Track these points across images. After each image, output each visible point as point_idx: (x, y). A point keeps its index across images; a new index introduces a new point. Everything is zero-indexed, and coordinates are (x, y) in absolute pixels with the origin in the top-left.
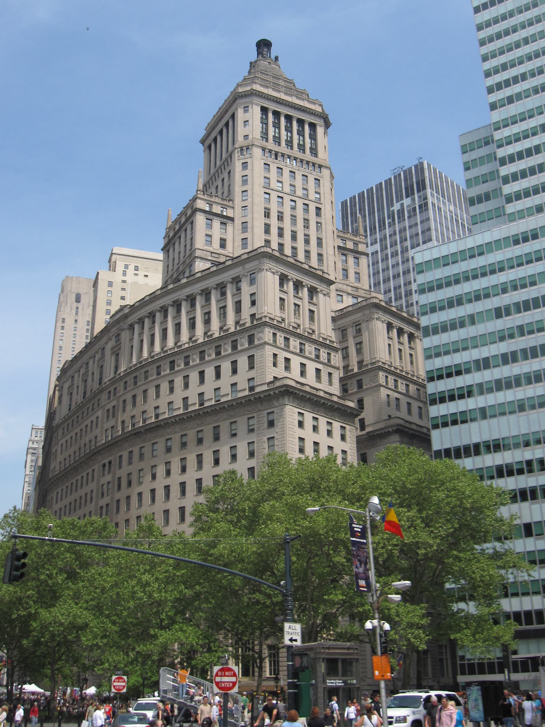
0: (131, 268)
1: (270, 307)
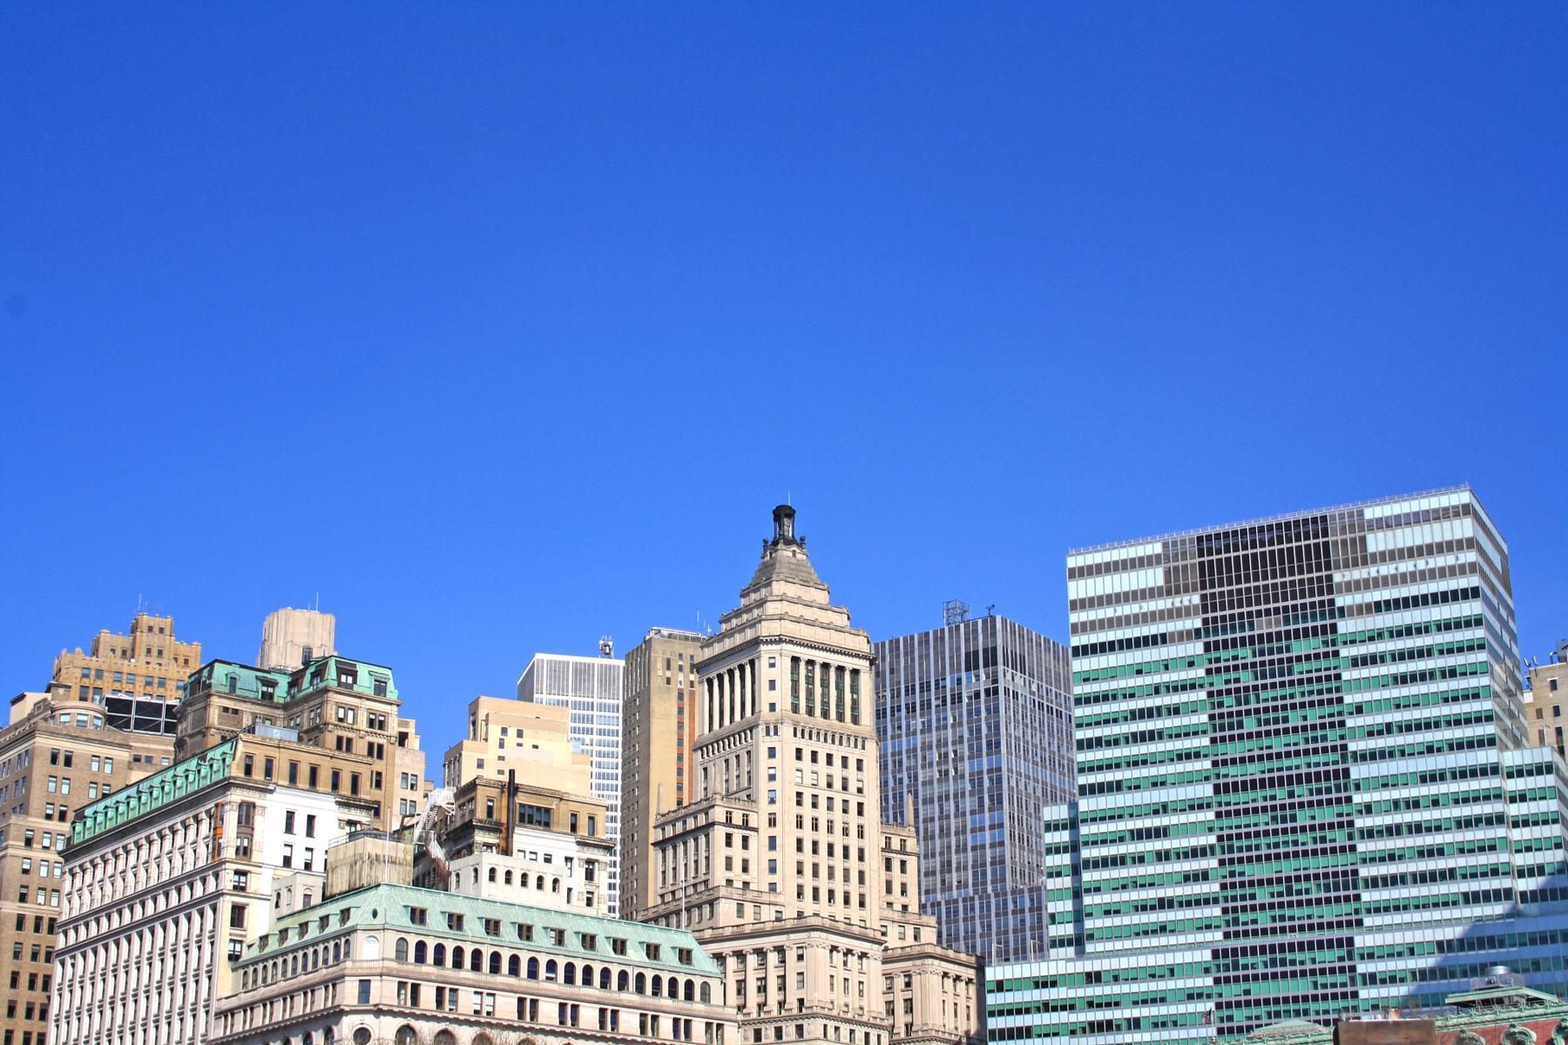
0: (512, 732)
1: (819, 994)
